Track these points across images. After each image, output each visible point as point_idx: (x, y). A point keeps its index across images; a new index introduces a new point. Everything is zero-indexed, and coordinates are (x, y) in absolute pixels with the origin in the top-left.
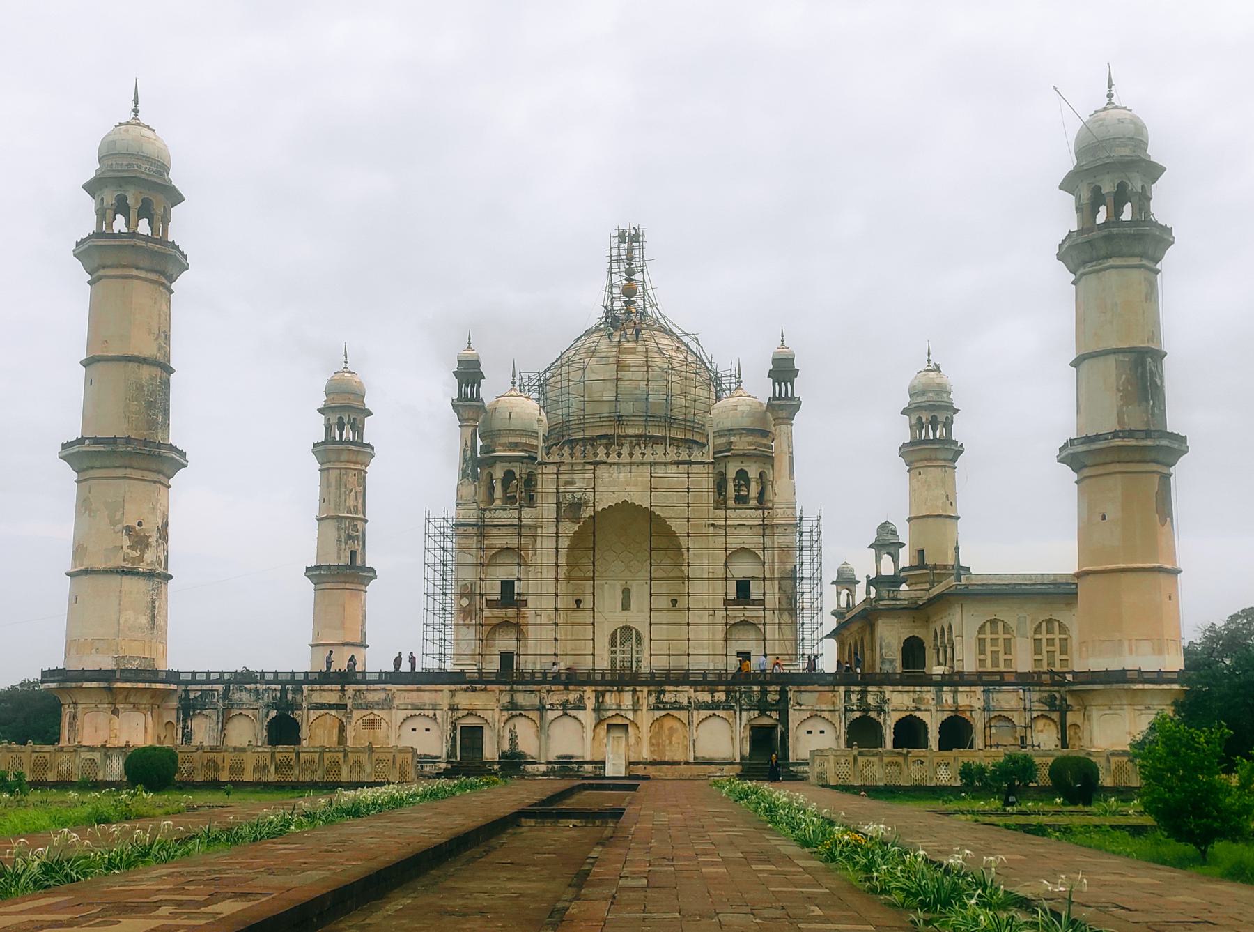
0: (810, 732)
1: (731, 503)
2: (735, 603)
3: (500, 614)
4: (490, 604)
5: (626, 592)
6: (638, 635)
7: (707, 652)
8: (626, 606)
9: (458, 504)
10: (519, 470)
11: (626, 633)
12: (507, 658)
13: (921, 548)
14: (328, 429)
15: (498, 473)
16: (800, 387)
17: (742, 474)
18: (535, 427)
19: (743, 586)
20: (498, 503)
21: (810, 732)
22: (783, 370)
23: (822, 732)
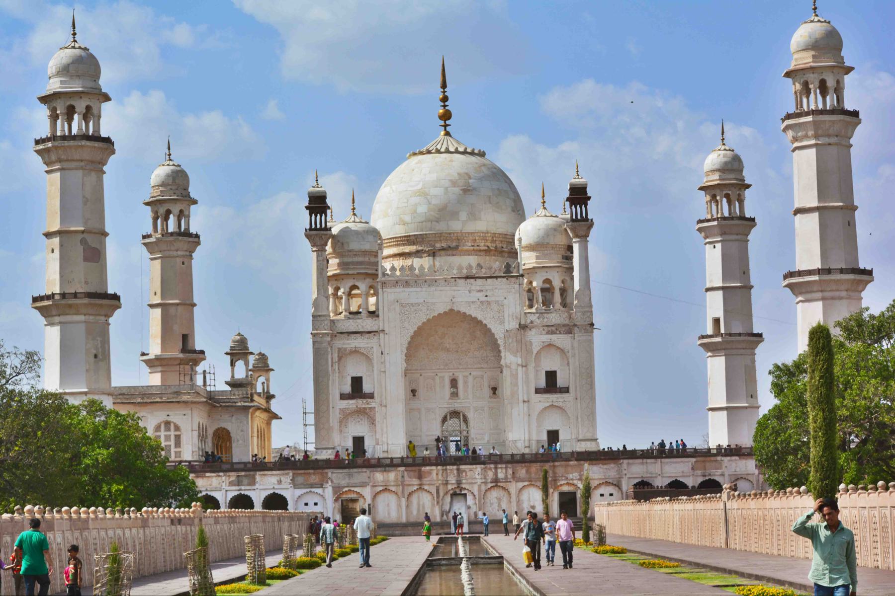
0: (602, 495)
3: (352, 404)
4: (343, 397)
5: (454, 383)
6: (466, 420)
7: (522, 433)
8: (455, 395)
9: (313, 316)
10: (363, 286)
12: (359, 442)
13: (716, 316)
14: (155, 219)
16: (593, 210)
17: (547, 281)
19: (551, 376)
21: (602, 495)
23: (611, 495)
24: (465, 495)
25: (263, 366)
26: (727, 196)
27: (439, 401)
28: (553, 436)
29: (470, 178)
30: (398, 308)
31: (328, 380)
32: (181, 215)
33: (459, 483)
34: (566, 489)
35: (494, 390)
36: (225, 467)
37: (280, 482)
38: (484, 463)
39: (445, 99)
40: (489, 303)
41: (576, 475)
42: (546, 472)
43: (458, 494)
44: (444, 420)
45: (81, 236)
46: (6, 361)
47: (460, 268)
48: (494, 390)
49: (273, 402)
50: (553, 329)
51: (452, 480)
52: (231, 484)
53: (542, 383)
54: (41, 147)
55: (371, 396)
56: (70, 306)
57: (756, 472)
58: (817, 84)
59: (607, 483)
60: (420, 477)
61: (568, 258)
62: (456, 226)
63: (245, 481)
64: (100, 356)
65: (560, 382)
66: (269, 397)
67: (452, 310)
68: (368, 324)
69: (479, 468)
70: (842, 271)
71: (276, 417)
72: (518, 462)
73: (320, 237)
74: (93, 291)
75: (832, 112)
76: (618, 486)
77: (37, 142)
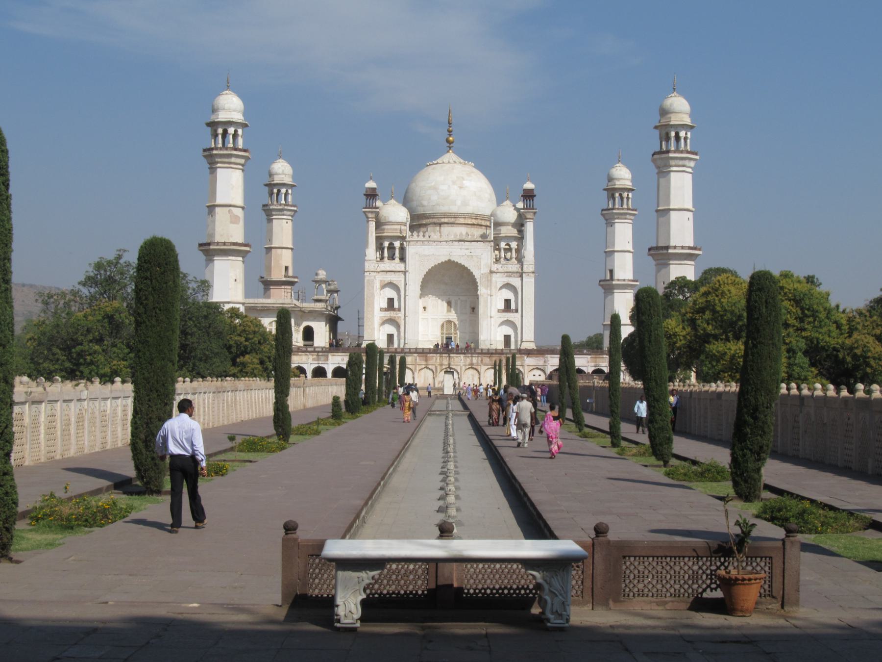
1: (502, 260)
2: (504, 311)
4: (382, 310)
10: (397, 244)
12: (390, 337)
14: (271, 194)
20: (386, 259)
24: (452, 373)
26: (621, 195)
28: (507, 338)
29: (463, 179)
31: (374, 298)
33: (449, 365)
35: (473, 309)
36: (309, 349)
37: (343, 360)
40: (472, 256)
42: (500, 361)
43: (449, 371)
44: (443, 326)
45: (228, 208)
46: (190, 286)
47: (456, 235)
48: (473, 309)
50: (509, 274)
51: (446, 362)
52: (313, 359)
53: (502, 306)
54: (206, 154)
56: (221, 250)
58: (673, 134)
59: (538, 369)
60: (426, 360)
61: (521, 232)
62: (454, 209)
63: (322, 358)
67: (449, 260)
68: (400, 266)
69: (462, 356)
70: (683, 248)
71: (340, 319)
73: (372, 212)
74: (235, 241)
75: (682, 152)
76: (544, 371)
77: (205, 150)
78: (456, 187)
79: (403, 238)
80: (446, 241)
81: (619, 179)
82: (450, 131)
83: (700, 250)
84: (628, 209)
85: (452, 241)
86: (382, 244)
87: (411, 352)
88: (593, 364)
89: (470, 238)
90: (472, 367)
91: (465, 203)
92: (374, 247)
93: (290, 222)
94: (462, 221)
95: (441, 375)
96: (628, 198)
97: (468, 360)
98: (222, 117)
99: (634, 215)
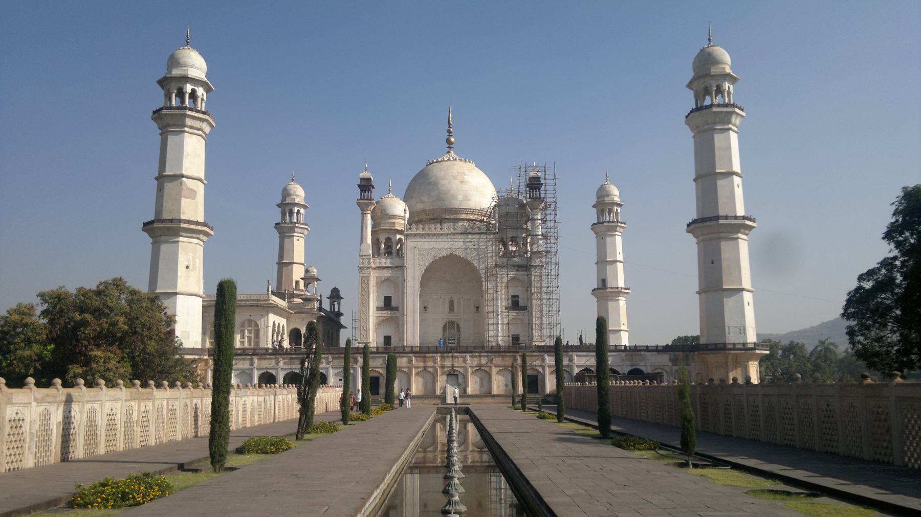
4: (379, 309)
5: (451, 303)
11: (451, 325)
14: (284, 215)
15: (382, 239)
18: (403, 214)
22: (534, 184)
25: (335, 295)
27: (440, 315)
30: (417, 252)
32: (298, 212)
34: (530, 372)
38: (471, 352)
39: (449, 132)
41: (538, 363)
48: (478, 308)
49: (342, 318)
55: (396, 309)
56: (168, 228)
57: (670, 364)
60: (424, 362)
62: (456, 204)
64: (191, 267)
65: (521, 303)
66: (339, 314)
67: (451, 254)
68: (397, 262)
69: (468, 356)
72: (495, 352)
78: (457, 182)
79: (401, 232)
80: (448, 234)
81: (608, 195)
82: (449, 132)
83: (754, 221)
84: (618, 222)
85: (454, 234)
86: (378, 240)
87: (403, 351)
88: (629, 363)
89: (470, 230)
90: (479, 369)
91: (466, 198)
92: (369, 241)
93: (302, 241)
94: (463, 216)
95: (441, 380)
96: (617, 213)
97: (476, 362)
98: (176, 72)
99: (624, 228)
